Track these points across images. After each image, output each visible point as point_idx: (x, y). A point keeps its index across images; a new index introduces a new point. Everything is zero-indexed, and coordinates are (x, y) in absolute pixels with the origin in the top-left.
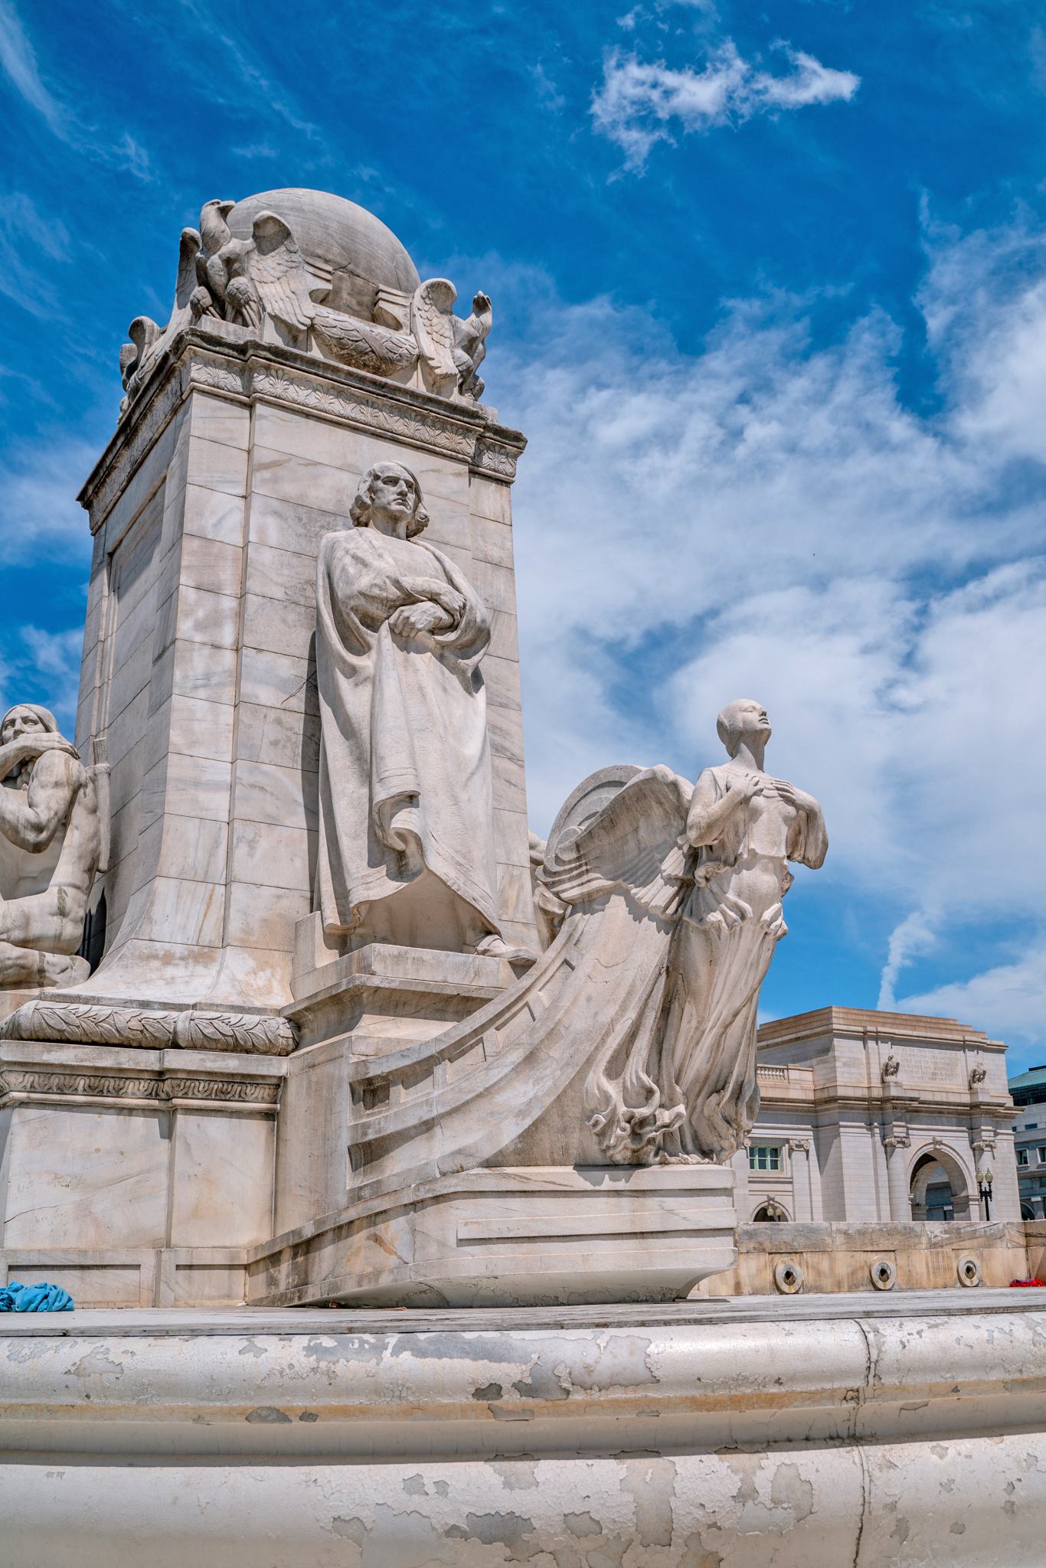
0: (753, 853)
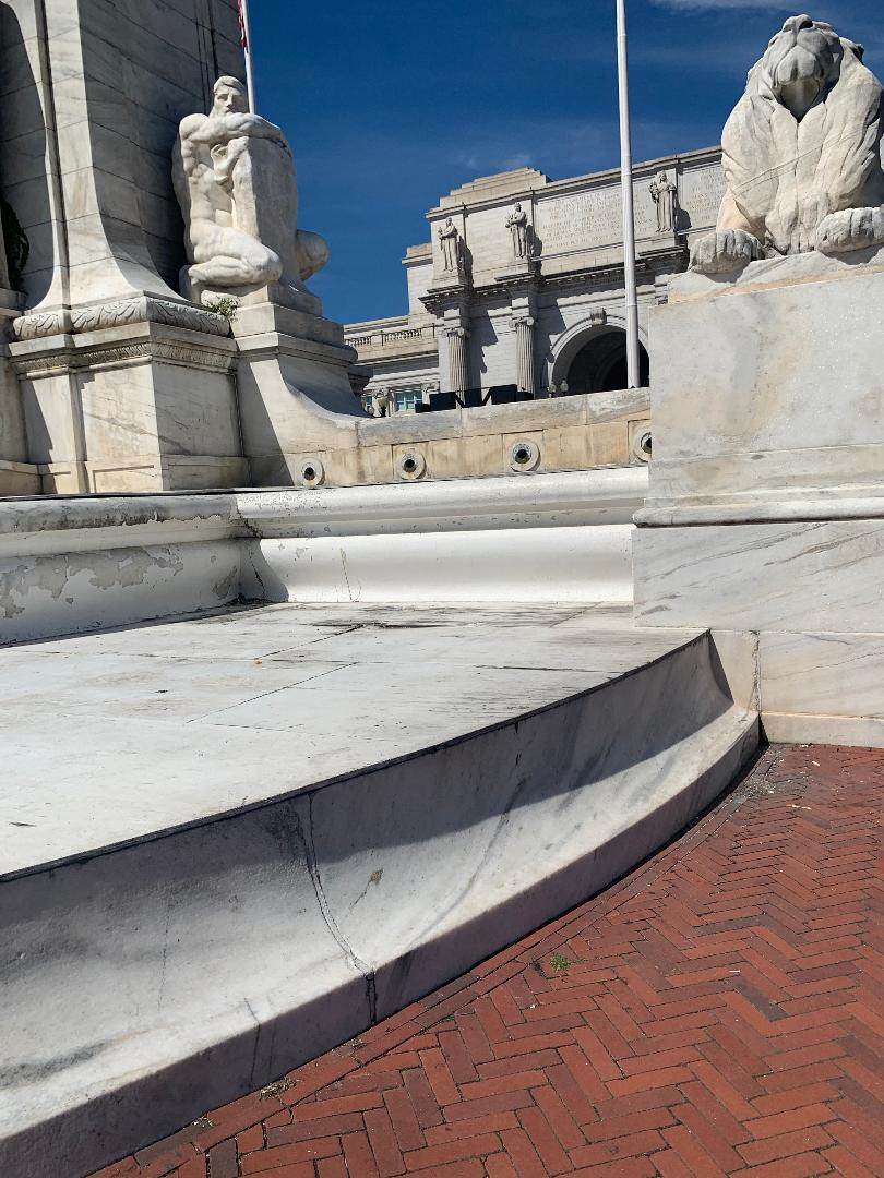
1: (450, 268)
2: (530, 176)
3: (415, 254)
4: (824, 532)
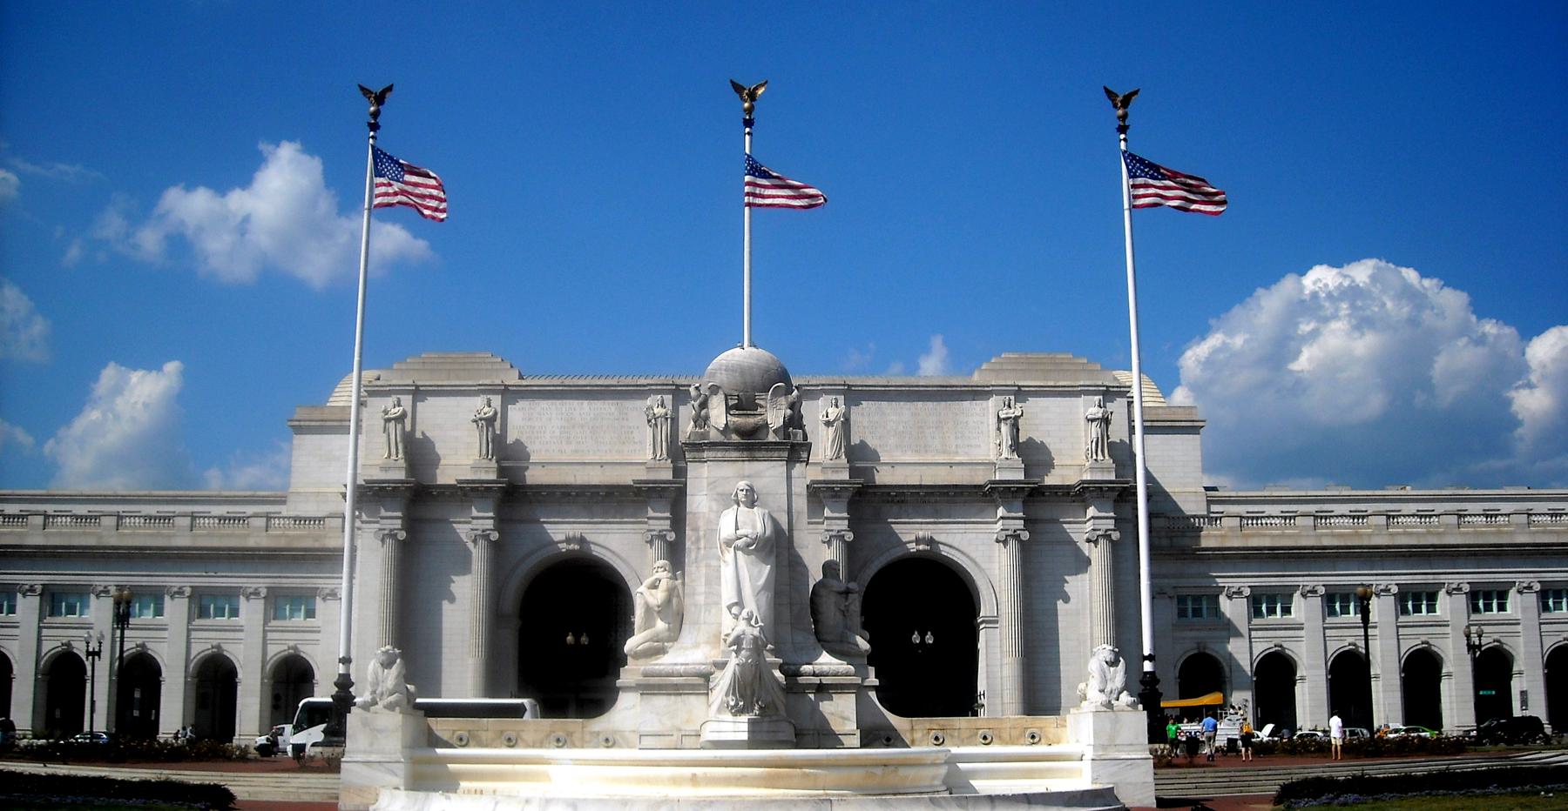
0: (744, 649)
1: (394, 457)
2: (495, 367)
3: (307, 417)
4: (1130, 762)
